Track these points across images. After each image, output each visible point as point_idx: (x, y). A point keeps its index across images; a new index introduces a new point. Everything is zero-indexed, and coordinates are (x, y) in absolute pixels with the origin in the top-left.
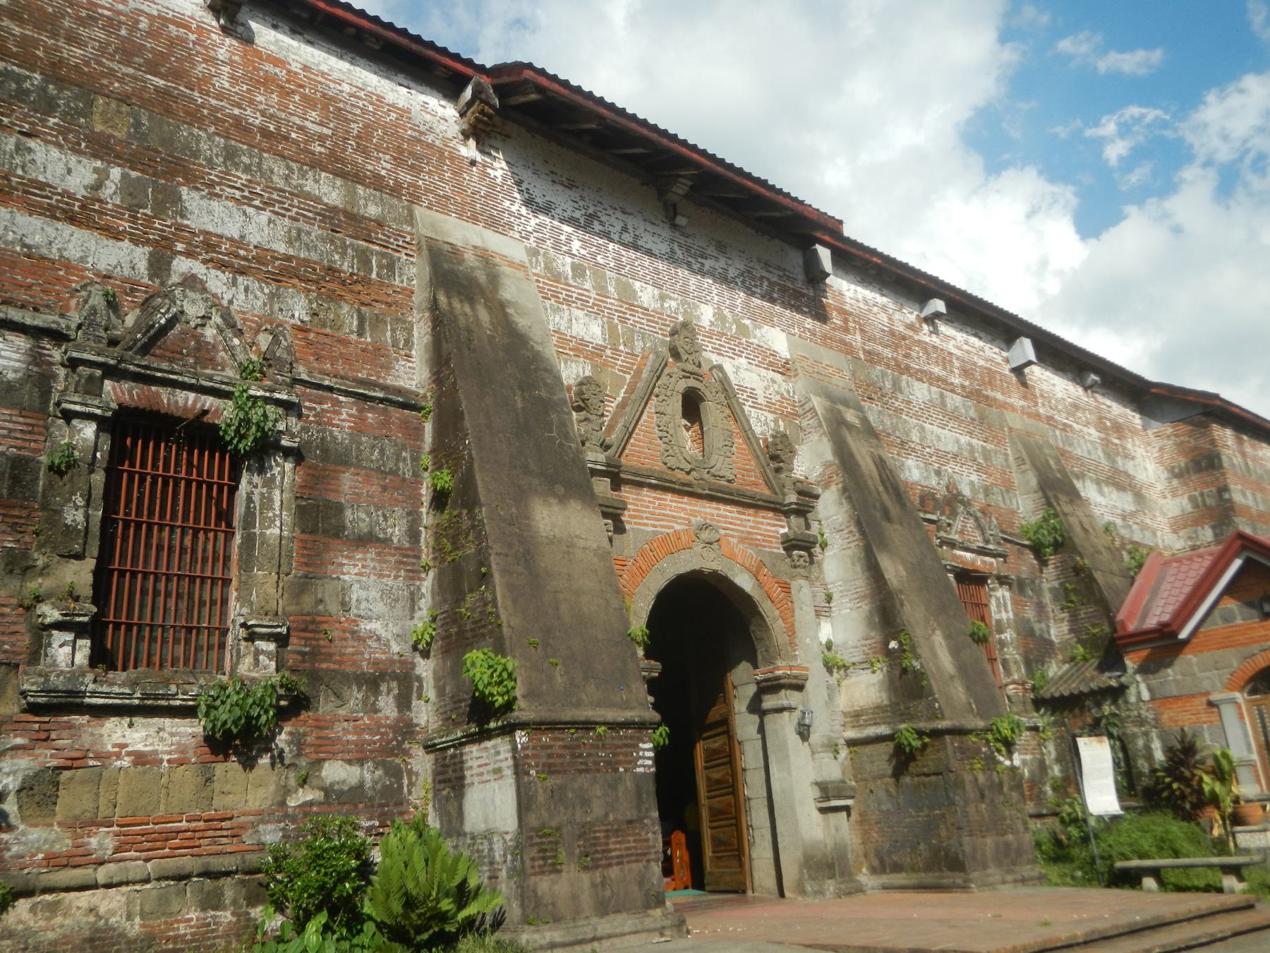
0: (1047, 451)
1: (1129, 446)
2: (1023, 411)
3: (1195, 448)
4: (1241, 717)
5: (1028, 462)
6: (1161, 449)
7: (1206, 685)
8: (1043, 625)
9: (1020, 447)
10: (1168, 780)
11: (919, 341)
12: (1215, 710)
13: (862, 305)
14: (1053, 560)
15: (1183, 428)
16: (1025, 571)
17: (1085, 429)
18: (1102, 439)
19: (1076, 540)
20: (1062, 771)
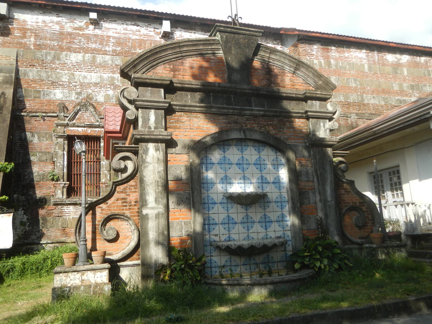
11: (83, 34)
13: (40, 24)
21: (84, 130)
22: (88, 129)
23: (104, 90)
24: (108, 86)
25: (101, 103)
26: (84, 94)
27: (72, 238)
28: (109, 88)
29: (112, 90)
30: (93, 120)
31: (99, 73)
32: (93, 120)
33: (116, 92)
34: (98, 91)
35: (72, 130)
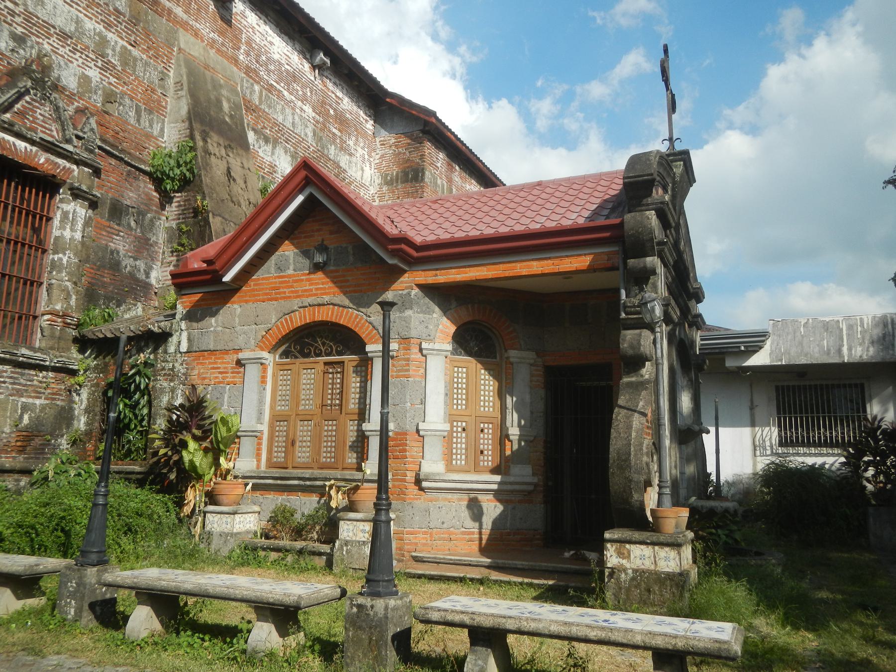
0: (224, 92)
1: (351, 143)
2: (212, 44)
4: (263, 380)
6: (382, 156)
7: (240, 341)
8: (141, 264)
9: (184, 71)
12: (242, 370)
14: (178, 197)
15: (405, 141)
16: (130, 197)
17: (299, 103)
19: (206, 180)
20: (87, 424)
21: (31, 150)
22: (40, 153)
23: (81, 60)
24: (91, 55)
25: (70, 92)
26: (32, 47)
28: (93, 60)
29: (98, 70)
30: (55, 133)
31: (76, 9)
32: (55, 133)
33: (107, 80)
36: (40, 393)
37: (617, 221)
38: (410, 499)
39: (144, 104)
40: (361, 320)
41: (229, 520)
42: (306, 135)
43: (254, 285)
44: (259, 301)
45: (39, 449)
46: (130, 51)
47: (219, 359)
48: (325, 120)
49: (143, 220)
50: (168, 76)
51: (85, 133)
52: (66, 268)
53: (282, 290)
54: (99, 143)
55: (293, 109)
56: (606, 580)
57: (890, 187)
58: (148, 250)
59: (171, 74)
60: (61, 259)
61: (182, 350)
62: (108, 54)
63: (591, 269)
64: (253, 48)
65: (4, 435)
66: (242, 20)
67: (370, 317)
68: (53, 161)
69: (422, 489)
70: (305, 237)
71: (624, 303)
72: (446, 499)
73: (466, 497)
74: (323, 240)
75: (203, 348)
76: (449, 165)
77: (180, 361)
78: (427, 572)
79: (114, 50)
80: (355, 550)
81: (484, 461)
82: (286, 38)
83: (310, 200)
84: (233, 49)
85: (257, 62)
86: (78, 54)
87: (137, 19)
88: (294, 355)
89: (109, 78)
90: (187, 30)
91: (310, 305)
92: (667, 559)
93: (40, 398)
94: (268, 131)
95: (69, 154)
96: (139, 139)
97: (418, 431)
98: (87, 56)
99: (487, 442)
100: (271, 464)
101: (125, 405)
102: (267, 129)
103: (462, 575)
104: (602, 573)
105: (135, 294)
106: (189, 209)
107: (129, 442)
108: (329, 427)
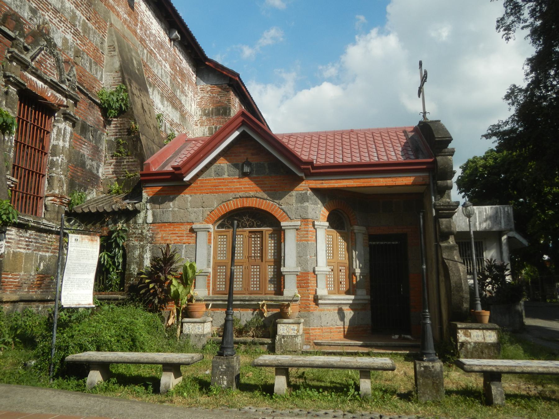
0: (133, 54)
1: (186, 88)
2: (125, 21)
3: (220, 102)
4: (210, 242)
5: (117, 50)
6: (202, 98)
7: (192, 217)
8: (94, 163)
10: (147, 281)
12: (194, 235)
14: (115, 121)
17: (164, 62)
18: (172, 74)
19: (135, 112)
21: (44, 87)
22: (49, 89)
23: (63, 28)
24: (68, 25)
26: (40, 17)
27: (8, 293)
32: (56, 76)
34: (56, 25)
35: (29, 79)
36: (48, 248)
37: (431, 160)
38: (312, 310)
39: (94, 59)
40: (275, 207)
41: (200, 327)
42: (167, 82)
43: (200, 183)
44: (205, 193)
45: (48, 286)
46: (87, 23)
47: (177, 228)
48: (175, 73)
49: (96, 135)
50: (104, 41)
51: (70, 77)
52: (61, 166)
53: (220, 187)
54: (77, 84)
55: (161, 66)
56: (459, 348)
57: (484, 138)
58: (98, 154)
59: (106, 40)
60: (58, 160)
61: (148, 222)
62: (77, 25)
63: (413, 185)
64: (143, 25)
65: (31, 277)
66: (139, 7)
67: (281, 205)
68: (54, 95)
69: (317, 304)
70: (235, 156)
71: (434, 204)
72: (328, 310)
73: (337, 308)
74: (247, 159)
75: (165, 221)
76: (240, 106)
77: (147, 228)
78: (335, 351)
79: (79, 22)
80: (289, 341)
81: (342, 287)
82: (158, 20)
83: (243, 135)
84: (135, 25)
85: (145, 34)
86: (62, 24)
87: (91, 3)
88: (227, 227)
89: (77, 40)
90: (113, 12)
91: (240, 197)
92: (490, 336)
93: (48, 252)
94: (150, 79)
95: (64, 91)
96: (92, 82)
97: (314, 272)
98: (67, 25)
99: (343, 277)
100: (215, 292)
101: (109, 256)
102: (150, 78)
103: (356, 351)
104: (456, 345)
105: (92, 183)
106: (124, 129)
107: (111, 280)
108: (255, 270)
